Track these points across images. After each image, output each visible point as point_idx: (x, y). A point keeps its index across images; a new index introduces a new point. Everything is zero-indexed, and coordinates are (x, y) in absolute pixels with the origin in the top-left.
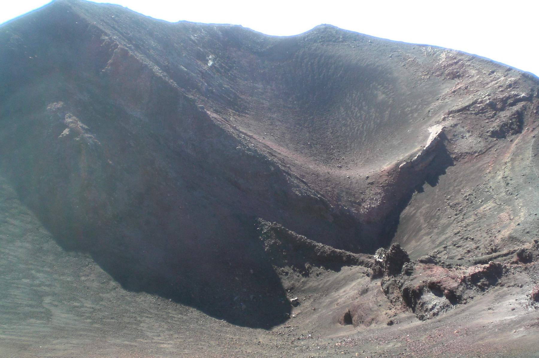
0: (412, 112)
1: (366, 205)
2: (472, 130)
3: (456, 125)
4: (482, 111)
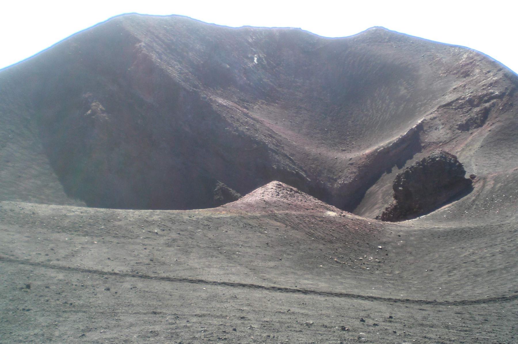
0: (421, 106)
1: (340, 181)
2: (446, 123)
3: (435, 118)
4: (461, 107)
